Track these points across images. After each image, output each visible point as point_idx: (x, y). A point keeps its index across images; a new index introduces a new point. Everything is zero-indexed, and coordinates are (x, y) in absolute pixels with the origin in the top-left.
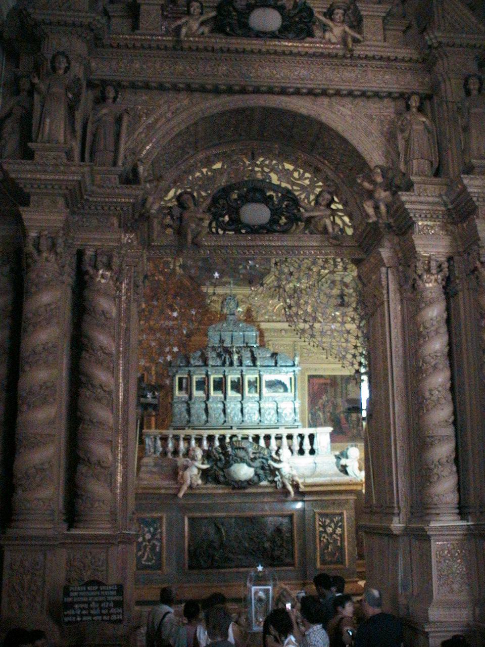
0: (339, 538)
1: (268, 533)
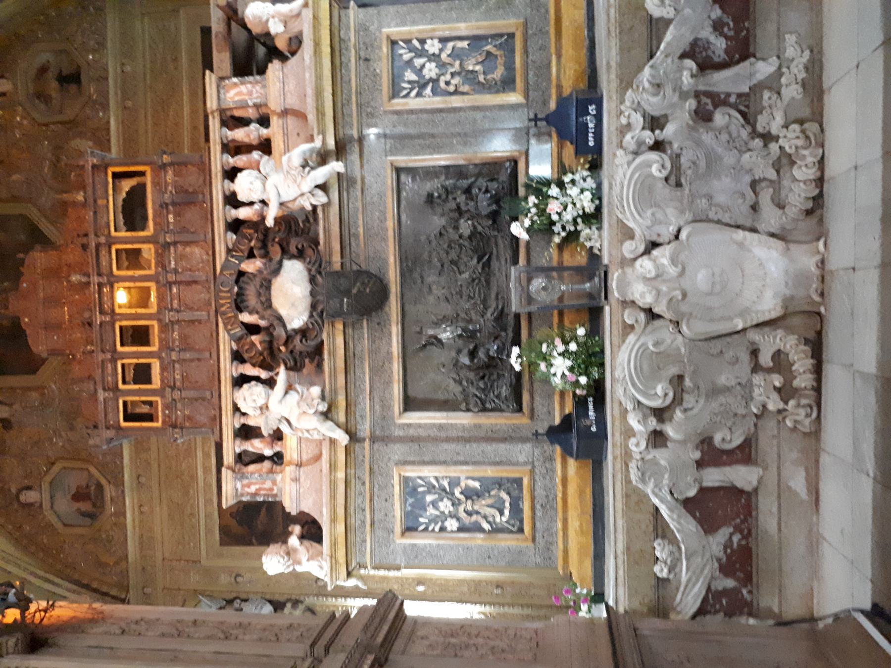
0: (450, 45)
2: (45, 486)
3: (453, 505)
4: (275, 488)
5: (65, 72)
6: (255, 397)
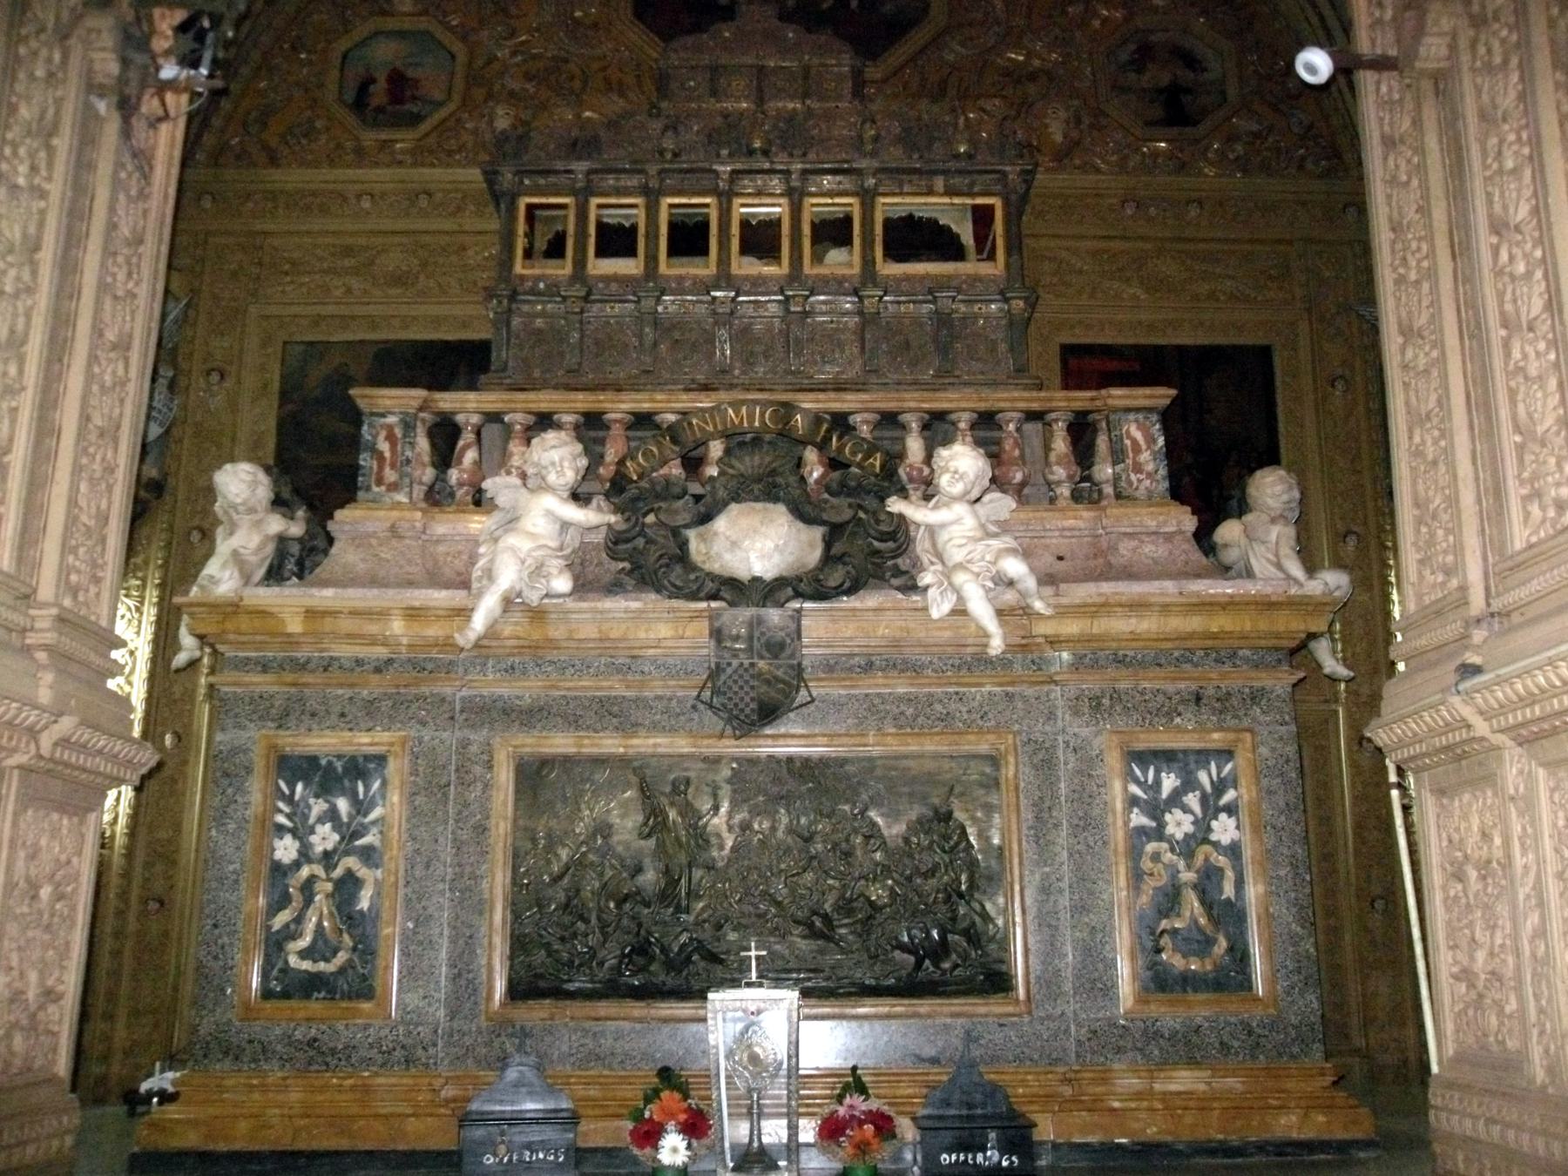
1: (893, 830)
2: (423, 23)
3: (327, 855)
4: (383, 488)
5: (1186, 99)
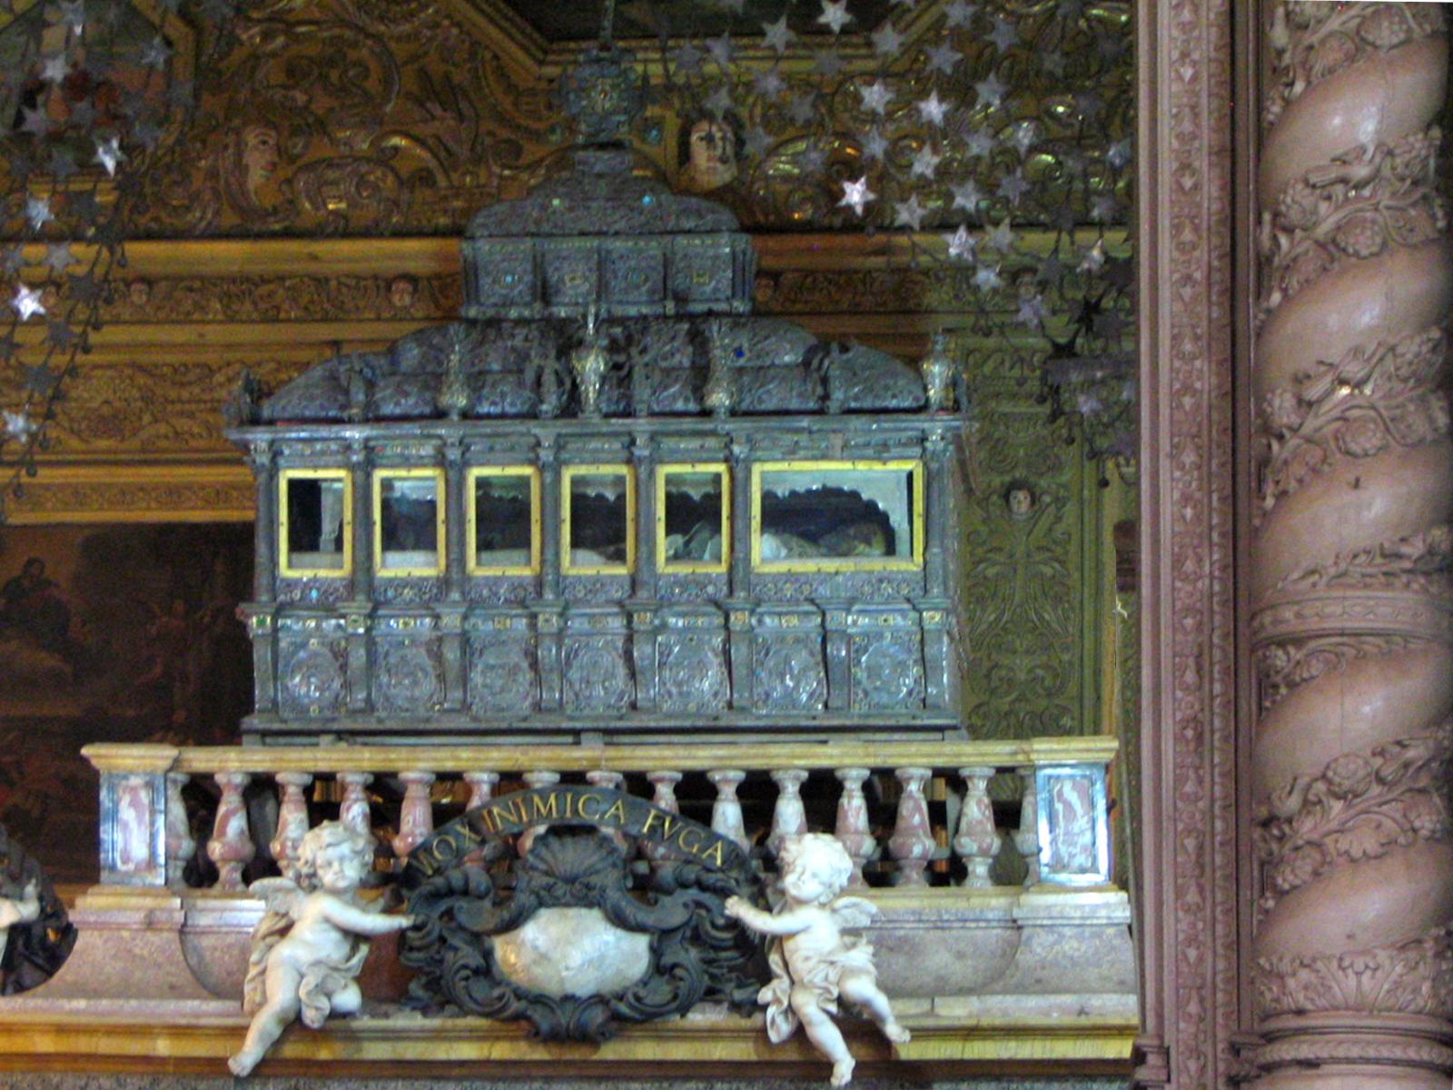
6: (336, 865)
